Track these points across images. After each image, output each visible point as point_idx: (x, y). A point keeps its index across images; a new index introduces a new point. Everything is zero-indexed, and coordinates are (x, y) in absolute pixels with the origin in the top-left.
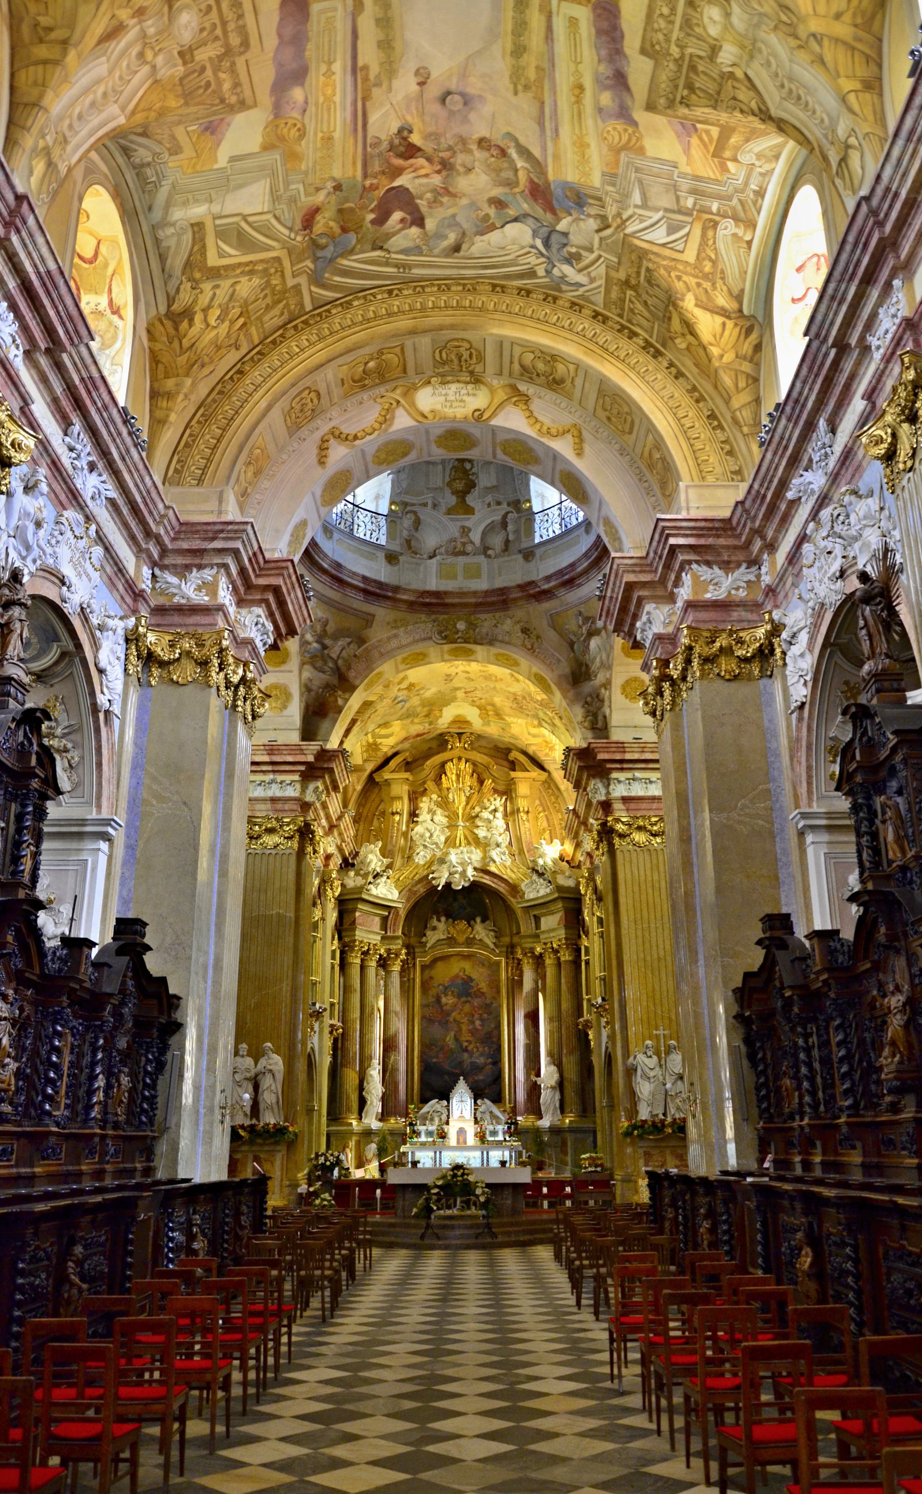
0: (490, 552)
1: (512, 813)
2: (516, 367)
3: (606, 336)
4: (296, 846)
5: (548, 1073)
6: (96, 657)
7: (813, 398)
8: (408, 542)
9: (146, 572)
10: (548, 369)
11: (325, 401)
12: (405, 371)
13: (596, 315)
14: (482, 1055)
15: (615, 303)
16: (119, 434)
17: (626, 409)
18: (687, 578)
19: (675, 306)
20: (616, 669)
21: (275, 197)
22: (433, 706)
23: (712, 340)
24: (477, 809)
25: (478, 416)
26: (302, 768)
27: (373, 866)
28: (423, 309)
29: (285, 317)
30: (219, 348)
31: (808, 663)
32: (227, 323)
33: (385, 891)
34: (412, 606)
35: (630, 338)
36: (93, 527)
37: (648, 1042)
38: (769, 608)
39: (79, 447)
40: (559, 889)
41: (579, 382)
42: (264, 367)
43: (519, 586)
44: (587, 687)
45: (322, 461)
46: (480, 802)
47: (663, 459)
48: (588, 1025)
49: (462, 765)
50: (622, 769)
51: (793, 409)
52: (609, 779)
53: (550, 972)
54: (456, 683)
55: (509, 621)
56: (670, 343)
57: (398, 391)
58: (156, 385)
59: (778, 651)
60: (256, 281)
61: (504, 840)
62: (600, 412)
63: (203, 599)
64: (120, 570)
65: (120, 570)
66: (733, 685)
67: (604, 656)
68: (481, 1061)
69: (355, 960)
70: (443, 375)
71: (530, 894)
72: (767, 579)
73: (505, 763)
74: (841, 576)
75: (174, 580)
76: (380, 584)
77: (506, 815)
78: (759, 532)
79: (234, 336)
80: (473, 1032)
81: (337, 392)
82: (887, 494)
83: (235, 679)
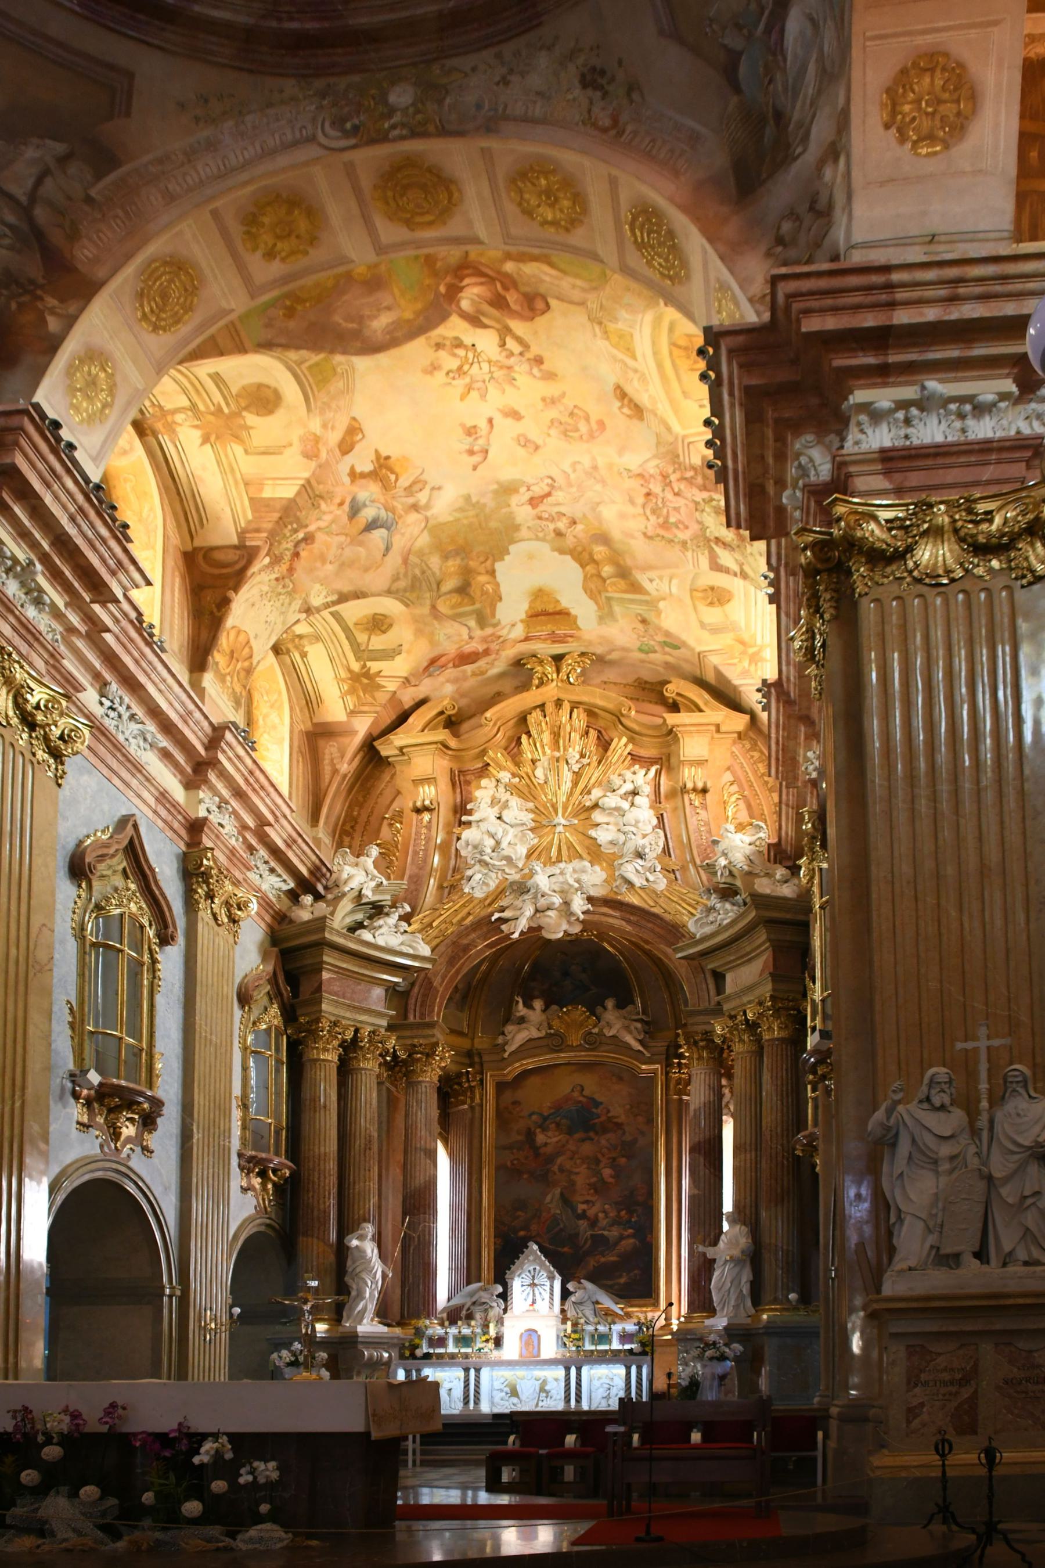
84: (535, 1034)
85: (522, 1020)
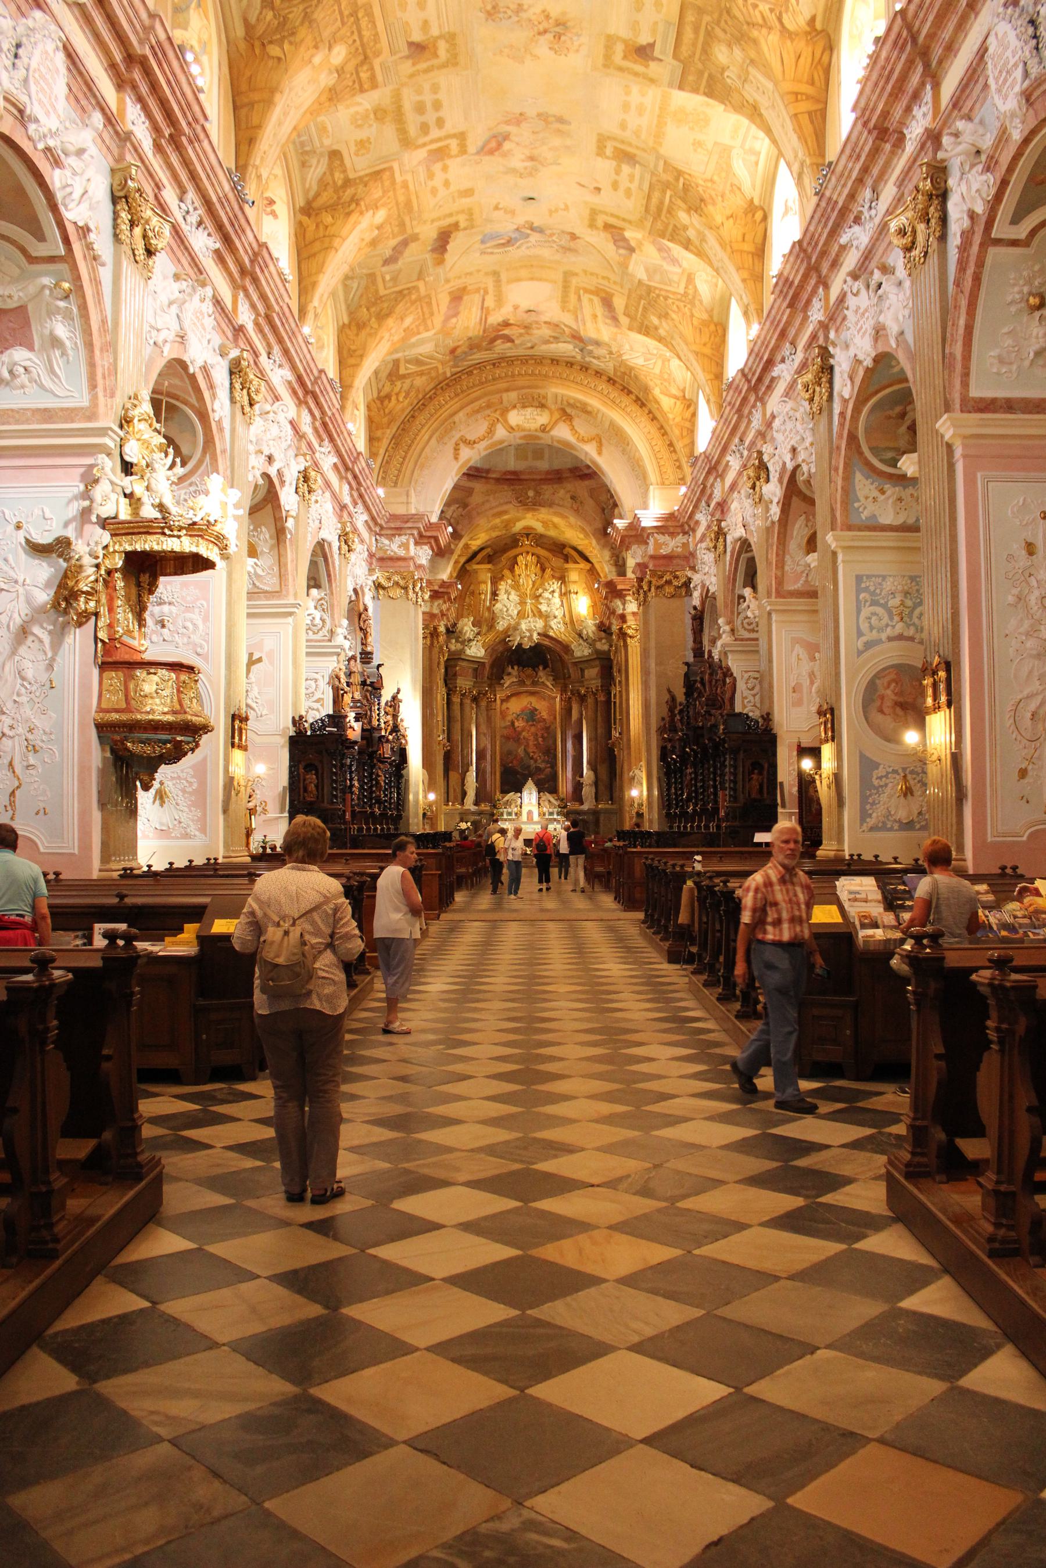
3: (614, 394)
21: (436, 346)
25: (543, 429)
28: (513, 376)
33: (476, 651)
40: (597, 652)
42: (425, 414)
45: (456, 458)
46: (542, 584)
49: (529, 558)
60: (424, 378)
61: (559, 613)
63: (402, 553)
68: (542, 766)
69: (456, 699)
75: (387, 542)
76: (477, 469)
77: (561, 595)
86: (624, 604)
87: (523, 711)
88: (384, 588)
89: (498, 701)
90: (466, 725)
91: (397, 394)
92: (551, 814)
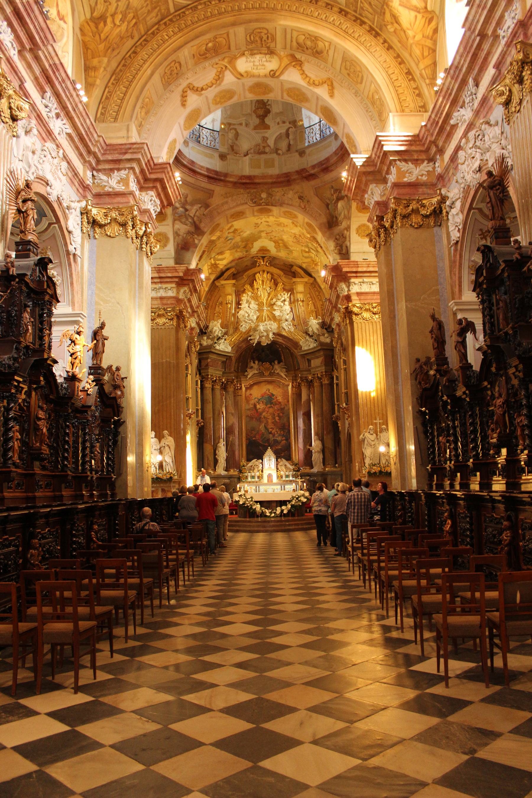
0: (279, 152)
1: (294, 302)
2: (294, 44)
3: (346, 24)
4: (175, 324)
5: (316, 444)
6: (66, 224)
7: (466, 66)
8: (232, 147)
9: (89, 174)
10: (313, 45)
11: (184, 68)
12: (229, 48)
13: (341, 11)
14: (280, 435)
15: (352, 4)
16: (72, 96)
17: (359, 69)
18: (393, 170)
19: (388, 5)
20: (353, 219)
22: (248, 243)
23: (409, 26)
24: (274, 300)
25: (273, 74)
26: (177, 280)
27: (216, 333)
28: (240, 9)
29: (159, 17)
30: (122, 38)
31: (460, 219)
32: (126, 23)
33: (224, 346)
34: (235, 184)
35: (361, 25)
36: (61, 152)
37: (371, 427)
38: (439, 187)
39: (50, 105)
40: (321, 344)
41: (331, 53)
42: (148, 49)
43: (297, 172)
44: (337, 230)
45: (183, 105)
46: (276, 296)
47: (380, 99)
48: (338, 418)
49: (265, 275)
50: (357, 277)
51: (455, 72)
52: (349, 283)
53: (317, 389)
54: (261, 228)
55: (291, 192)
56: (384, 28)
57: (226, 60)
58: (88, 63)
59: (444, 211)
61: (289, 317)
62: (344, 72)
63: (121, 188)
64: (76, 174)
65: (76, 174)
66: (419, 231)
67: (346, 213)
68: (279, 439)
69: (208, 385)
70: (251, 50)
71: (305, 348)
72: (439, 170)
73: (290, 273)
74: (479, 170)
75: (104, 178)
76: (216, 172)
77: (290, 303)
78: (434, 142)
79: (130, 30)
80: (275, 423)
81: (191, 62)
82: (505, 125)
83: (141, 233)
84: (256, 372)
85: (252, 367)
86: (348, 287)
87: (262, 396)
88: (101, 226)
89: (244, 389)
90: (218, 406)
91: (113, 16)
92: (287, 476)
